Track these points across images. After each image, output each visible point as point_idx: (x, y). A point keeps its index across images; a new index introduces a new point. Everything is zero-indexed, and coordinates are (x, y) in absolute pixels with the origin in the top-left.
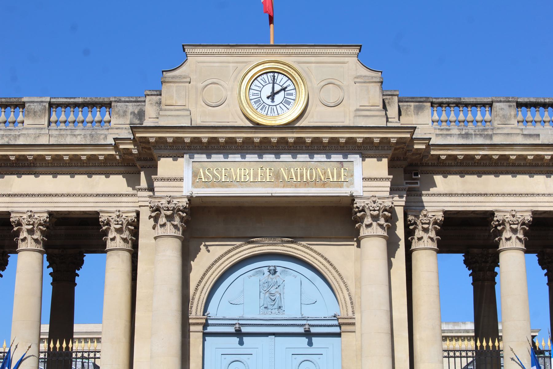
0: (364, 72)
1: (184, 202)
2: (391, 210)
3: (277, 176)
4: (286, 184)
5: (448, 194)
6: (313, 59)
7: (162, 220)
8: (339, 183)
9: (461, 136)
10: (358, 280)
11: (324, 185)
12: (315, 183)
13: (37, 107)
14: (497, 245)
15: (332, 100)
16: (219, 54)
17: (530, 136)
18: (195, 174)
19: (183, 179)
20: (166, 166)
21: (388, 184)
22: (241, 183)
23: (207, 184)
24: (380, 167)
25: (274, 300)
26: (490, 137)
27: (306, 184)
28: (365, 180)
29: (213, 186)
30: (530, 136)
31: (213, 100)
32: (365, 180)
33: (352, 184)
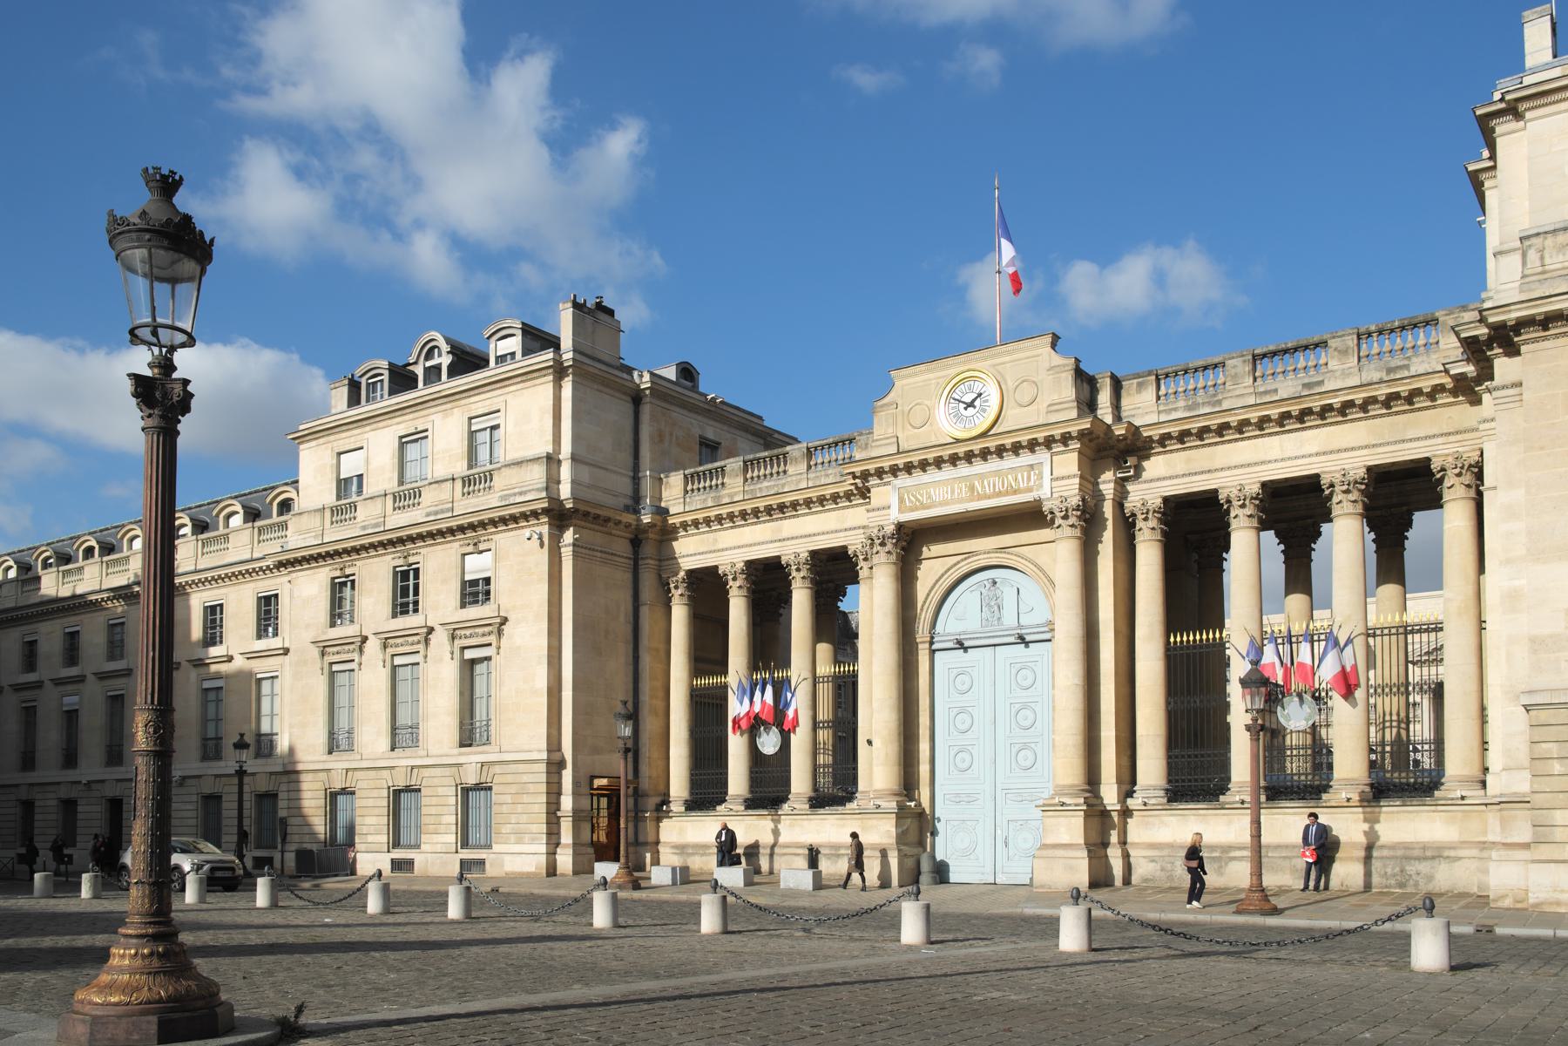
3: (972, 488)
4: (980, 498)
5: (1165, 476)
6: (1007, 359)
8: (1030, 490)
9: (1188, 408)
11: (1015, 492)
12: (1007, 493)
14: (1228, 525)
15: (1027, 399)
16: (916, 374)
17: (1266, 393)
18: (901, 500)
19: (893, 504)
21: (1077, 480)
22: (941, 504)
23: (912, 510)
26: (1219, 402)
27: (999, 494)
30: (1266, 393)
31: (918, 423)
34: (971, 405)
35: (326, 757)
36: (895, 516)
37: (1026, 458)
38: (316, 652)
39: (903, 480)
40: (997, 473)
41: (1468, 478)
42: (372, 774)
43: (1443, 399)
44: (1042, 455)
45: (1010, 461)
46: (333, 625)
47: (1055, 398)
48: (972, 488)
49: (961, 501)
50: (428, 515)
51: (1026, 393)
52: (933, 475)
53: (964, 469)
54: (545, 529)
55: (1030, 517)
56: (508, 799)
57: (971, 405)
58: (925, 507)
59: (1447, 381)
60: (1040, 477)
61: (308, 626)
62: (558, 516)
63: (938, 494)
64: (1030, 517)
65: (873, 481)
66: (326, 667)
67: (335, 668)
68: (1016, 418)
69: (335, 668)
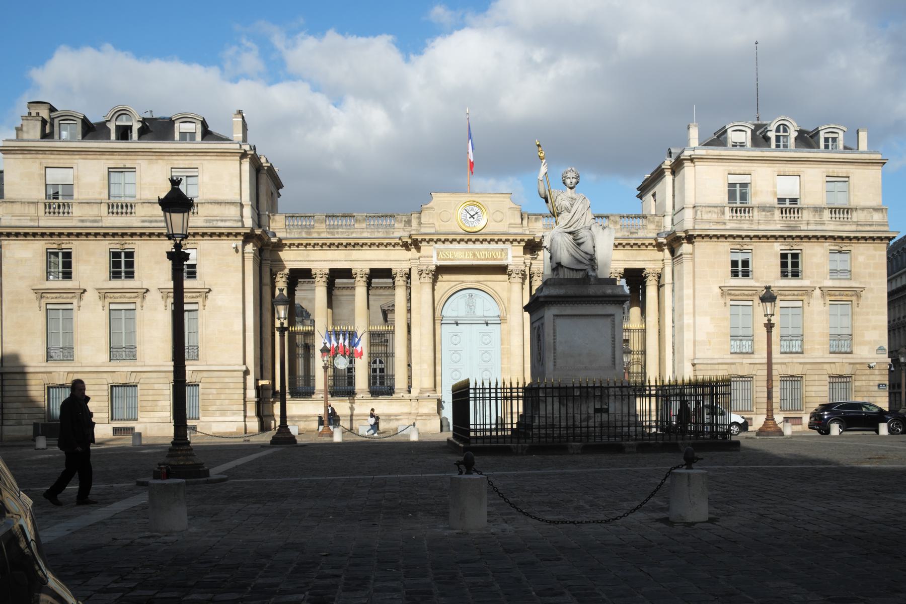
0: (513, 205)
1: (434, 268)
2: (524, 271)
3: (474, 255)
4: (478, 259)
7: (424, 275)
8: (502, 259)
10: (509, 300)
11: (495, 259)
12: (491, 259)
13: (361, 218)
15: (499, 219)
18: (438, 254)
19: (432, 256)
20: (425, 248)
22: (459, 259)
23: (443, 260)
24: (519, 249)
25: (470, 306)
27: (487, 259)
28: (513, 256)
29: (446, 260)
32: (513, 256)
33: (507, 259)
34: (472, 216)
35: (45, 364)
36: (435, 262)
37: (500, 245)
38: (33, 296)
39: (439, 245)
40: (487, 250)
41: (656, 278)
42: (95, 375)
43: (650, 248)
44: (508, 245)
45: (493, 245)
46: (47, 279)
47: (512, 221)
48: (474, 255)
49: (469, 259)
50: (143, 221)
51: (499, 216)
52: (455, 245)
53: (470, 245)
54: (240, 243)
55: (502, 270)
56: (214, 391)
57: (472, 216)
58: (450, 259)
59: (654, 243)
60: (507, 254)
61: (21, 278)
62: (248, 238)
63: (459, 255)
64: (502, 270)
65: (424, 243)
66: (43, 305)
67: (49, 307)
68: (494, 227)
69: (49, 307)
